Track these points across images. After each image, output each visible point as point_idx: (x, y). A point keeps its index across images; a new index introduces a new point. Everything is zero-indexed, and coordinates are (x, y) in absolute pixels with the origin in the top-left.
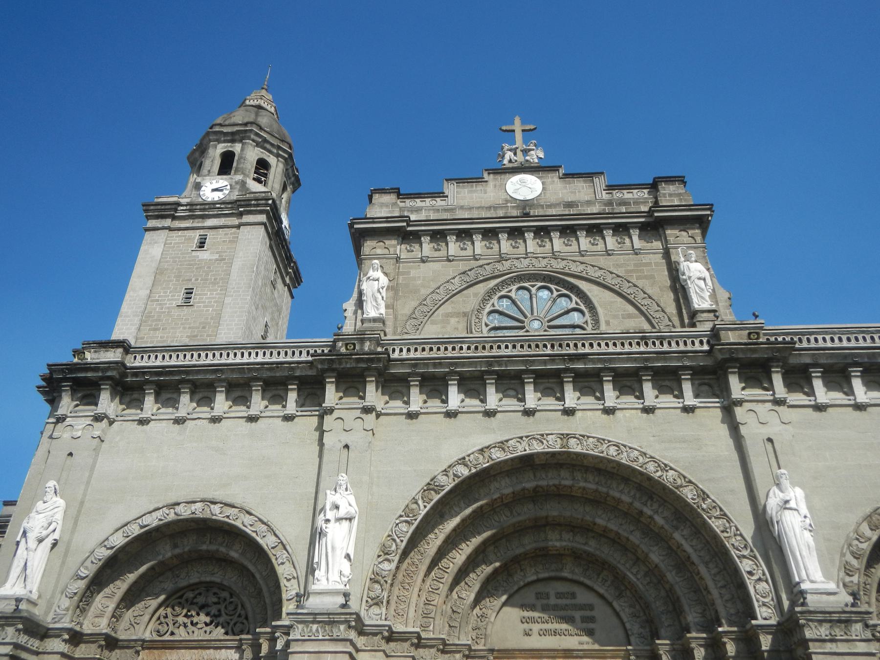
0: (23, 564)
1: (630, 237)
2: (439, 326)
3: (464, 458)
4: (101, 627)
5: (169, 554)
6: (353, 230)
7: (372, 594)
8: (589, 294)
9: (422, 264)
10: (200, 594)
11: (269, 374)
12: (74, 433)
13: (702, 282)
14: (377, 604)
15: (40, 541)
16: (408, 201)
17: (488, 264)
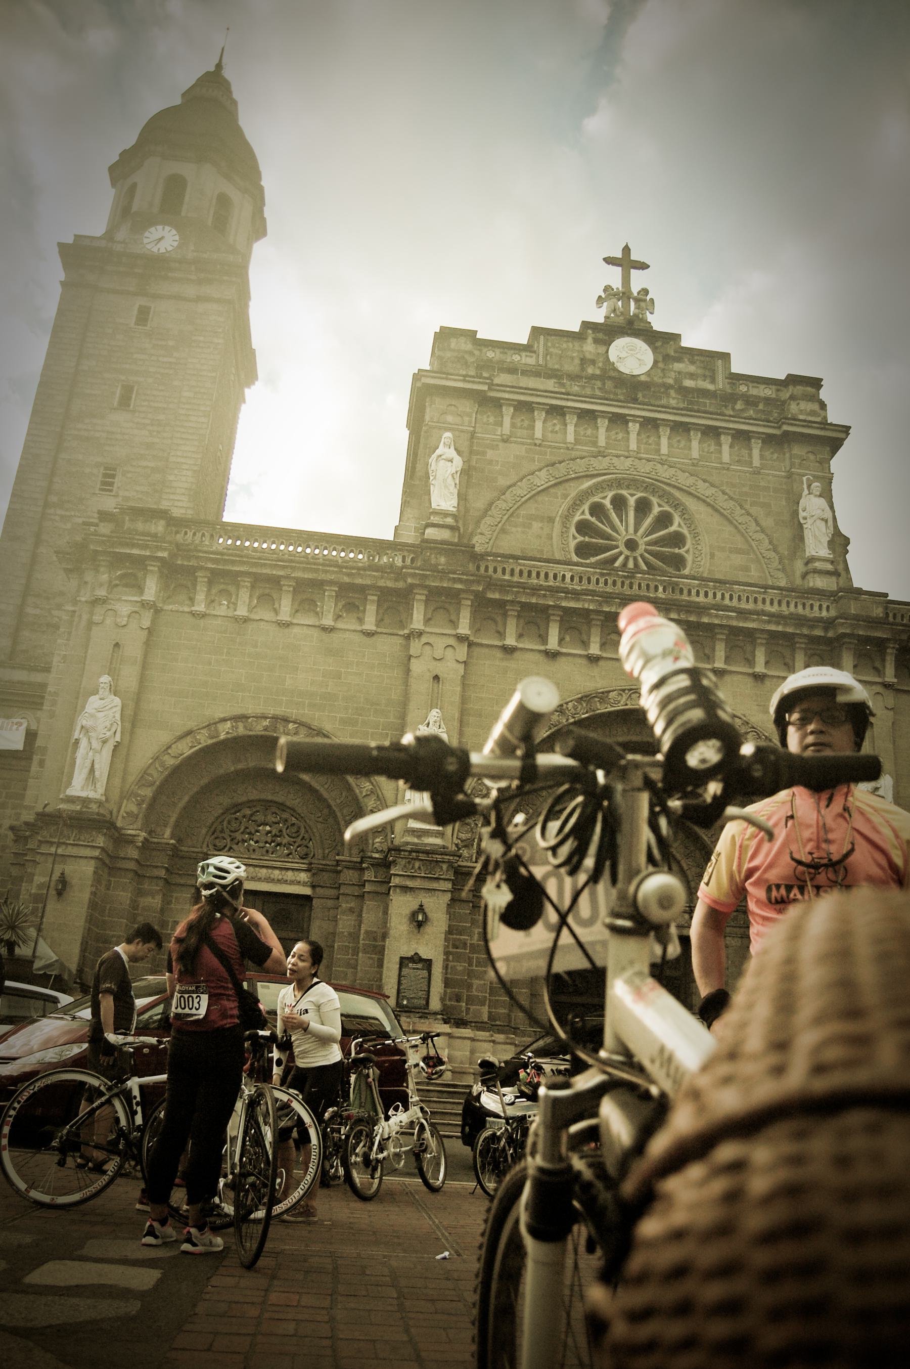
0: (88, 764)
1: (751, 449)
2: (519, 529)
3: (562, 705)
4: (166, 836)
5: (232, 769)
6: (419, 384)
7: (463, 836)
8: (697, 516)
9: (501, 444)
10: (258, 811)
11: (346, 579)
12: (118, 620)
13: (824, 523)
14: (465, 846)
15: (104, 742)
16: (485, 350)
17: (582, 458)
